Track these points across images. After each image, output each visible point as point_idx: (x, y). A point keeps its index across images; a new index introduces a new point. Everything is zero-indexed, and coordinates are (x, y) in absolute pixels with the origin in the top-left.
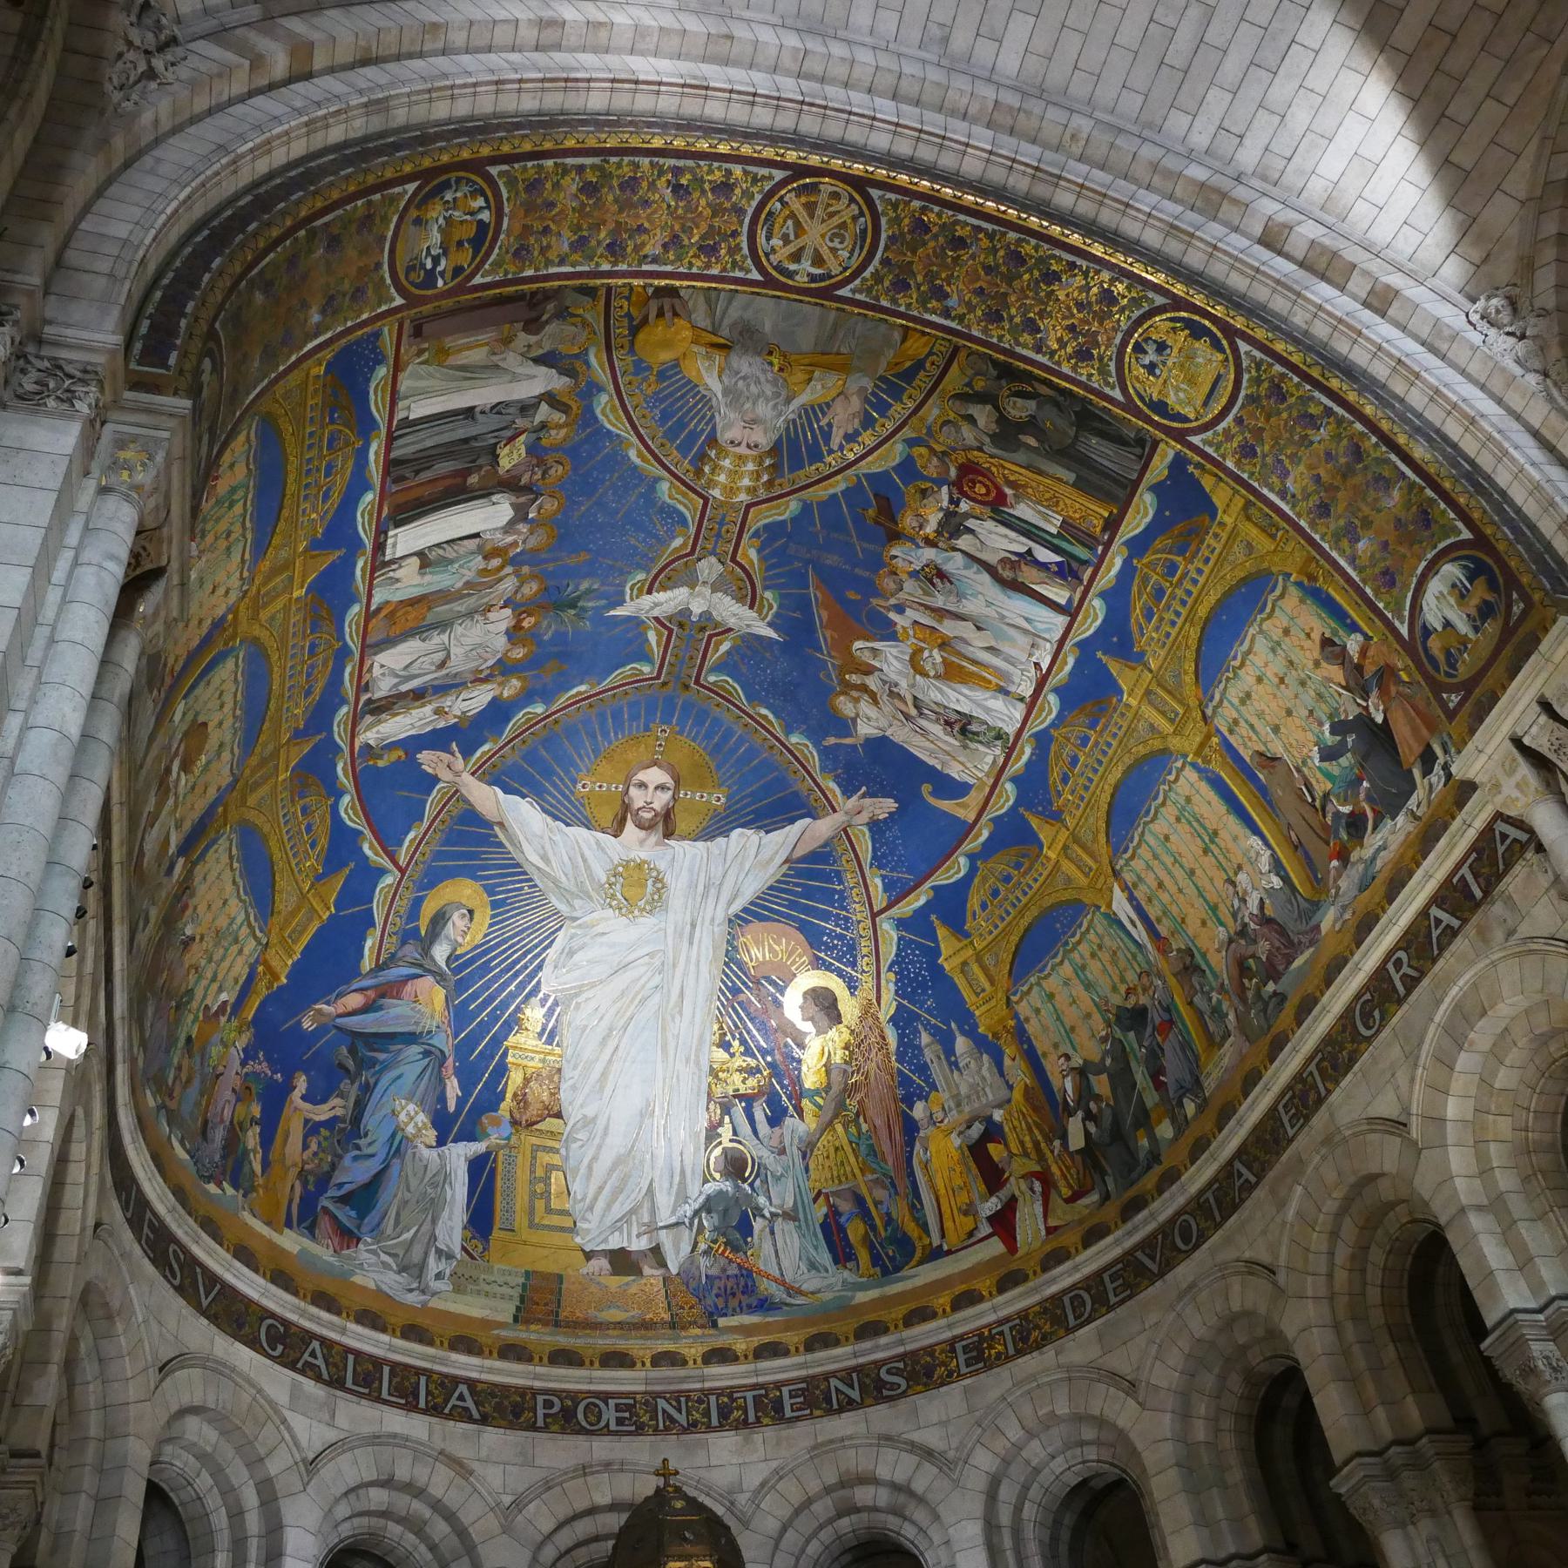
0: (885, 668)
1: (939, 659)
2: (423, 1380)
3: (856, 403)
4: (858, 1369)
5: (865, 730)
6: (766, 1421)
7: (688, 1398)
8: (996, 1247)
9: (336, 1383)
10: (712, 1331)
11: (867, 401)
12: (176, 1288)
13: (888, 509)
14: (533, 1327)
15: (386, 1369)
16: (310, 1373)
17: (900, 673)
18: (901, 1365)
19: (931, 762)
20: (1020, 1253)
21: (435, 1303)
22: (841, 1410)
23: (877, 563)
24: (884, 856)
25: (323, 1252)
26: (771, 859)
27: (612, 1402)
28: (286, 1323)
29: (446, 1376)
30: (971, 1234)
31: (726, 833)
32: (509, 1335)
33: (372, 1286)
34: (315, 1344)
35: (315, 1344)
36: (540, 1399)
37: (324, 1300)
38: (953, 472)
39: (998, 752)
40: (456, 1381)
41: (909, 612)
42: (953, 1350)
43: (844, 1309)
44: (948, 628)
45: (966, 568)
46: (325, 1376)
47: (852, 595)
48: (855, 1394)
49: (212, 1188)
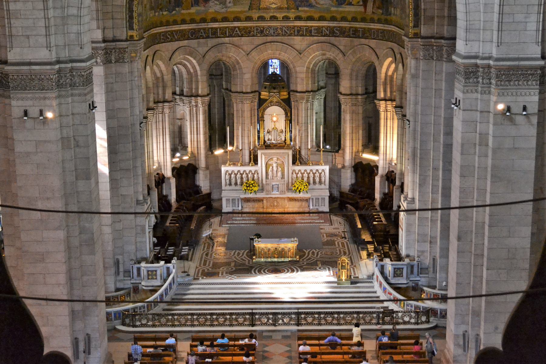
2: (227, 29)
4: (329, 27)
6: (308, 35)
7: (290, 27)
8: (362, 9)
9: (208, 37)
10: (296, 11)
12: (170, 42)
14: (253, 11)
15: (218, 29)
16: (201, 38)
18: (339, 29)
20: (367, 13)
21: (229, 10)
22: (324, 36)
25: (201, 8)
27: (272, 28)
28: (194, 29)
29: (232, 27)
30: (358, 2)
32: (248, 15)
33: (213, 11)
34: (202, 31)
35: (202, 31)
36: (255, 28)
37: (204, 20)
40: (235, 27)
42: (350, 30)
43: (328, 10)
46: (205, 37)
48: (328, 33)
49: (174, 12)
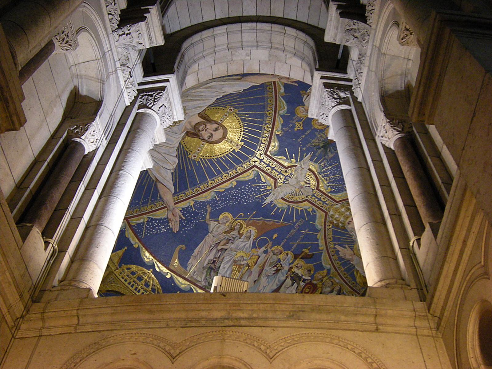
0: (241, 240)
1: (242, 263)
3: (348, 257)
5: (212, 224)
11: (349, 261)
13: (306, 258)
17: (238, 245)
19: (196, 251)
23: (287, 247)
24: (153, 224)
26: (160, 174)
31: (178, 156)
38: (315, 282)
39: (203, 283)
41: (264, 255)
44: (255, 270)
45: (279, 280)
47: (275, 236)
